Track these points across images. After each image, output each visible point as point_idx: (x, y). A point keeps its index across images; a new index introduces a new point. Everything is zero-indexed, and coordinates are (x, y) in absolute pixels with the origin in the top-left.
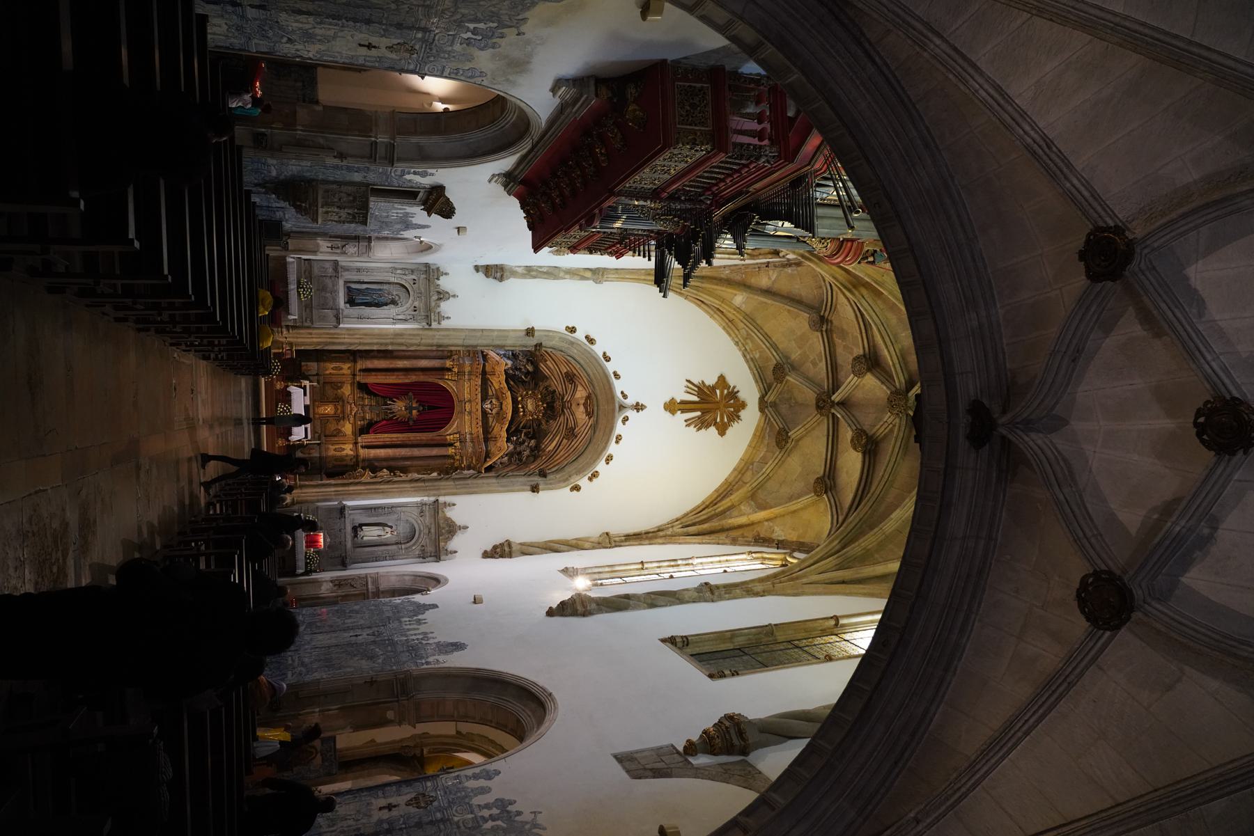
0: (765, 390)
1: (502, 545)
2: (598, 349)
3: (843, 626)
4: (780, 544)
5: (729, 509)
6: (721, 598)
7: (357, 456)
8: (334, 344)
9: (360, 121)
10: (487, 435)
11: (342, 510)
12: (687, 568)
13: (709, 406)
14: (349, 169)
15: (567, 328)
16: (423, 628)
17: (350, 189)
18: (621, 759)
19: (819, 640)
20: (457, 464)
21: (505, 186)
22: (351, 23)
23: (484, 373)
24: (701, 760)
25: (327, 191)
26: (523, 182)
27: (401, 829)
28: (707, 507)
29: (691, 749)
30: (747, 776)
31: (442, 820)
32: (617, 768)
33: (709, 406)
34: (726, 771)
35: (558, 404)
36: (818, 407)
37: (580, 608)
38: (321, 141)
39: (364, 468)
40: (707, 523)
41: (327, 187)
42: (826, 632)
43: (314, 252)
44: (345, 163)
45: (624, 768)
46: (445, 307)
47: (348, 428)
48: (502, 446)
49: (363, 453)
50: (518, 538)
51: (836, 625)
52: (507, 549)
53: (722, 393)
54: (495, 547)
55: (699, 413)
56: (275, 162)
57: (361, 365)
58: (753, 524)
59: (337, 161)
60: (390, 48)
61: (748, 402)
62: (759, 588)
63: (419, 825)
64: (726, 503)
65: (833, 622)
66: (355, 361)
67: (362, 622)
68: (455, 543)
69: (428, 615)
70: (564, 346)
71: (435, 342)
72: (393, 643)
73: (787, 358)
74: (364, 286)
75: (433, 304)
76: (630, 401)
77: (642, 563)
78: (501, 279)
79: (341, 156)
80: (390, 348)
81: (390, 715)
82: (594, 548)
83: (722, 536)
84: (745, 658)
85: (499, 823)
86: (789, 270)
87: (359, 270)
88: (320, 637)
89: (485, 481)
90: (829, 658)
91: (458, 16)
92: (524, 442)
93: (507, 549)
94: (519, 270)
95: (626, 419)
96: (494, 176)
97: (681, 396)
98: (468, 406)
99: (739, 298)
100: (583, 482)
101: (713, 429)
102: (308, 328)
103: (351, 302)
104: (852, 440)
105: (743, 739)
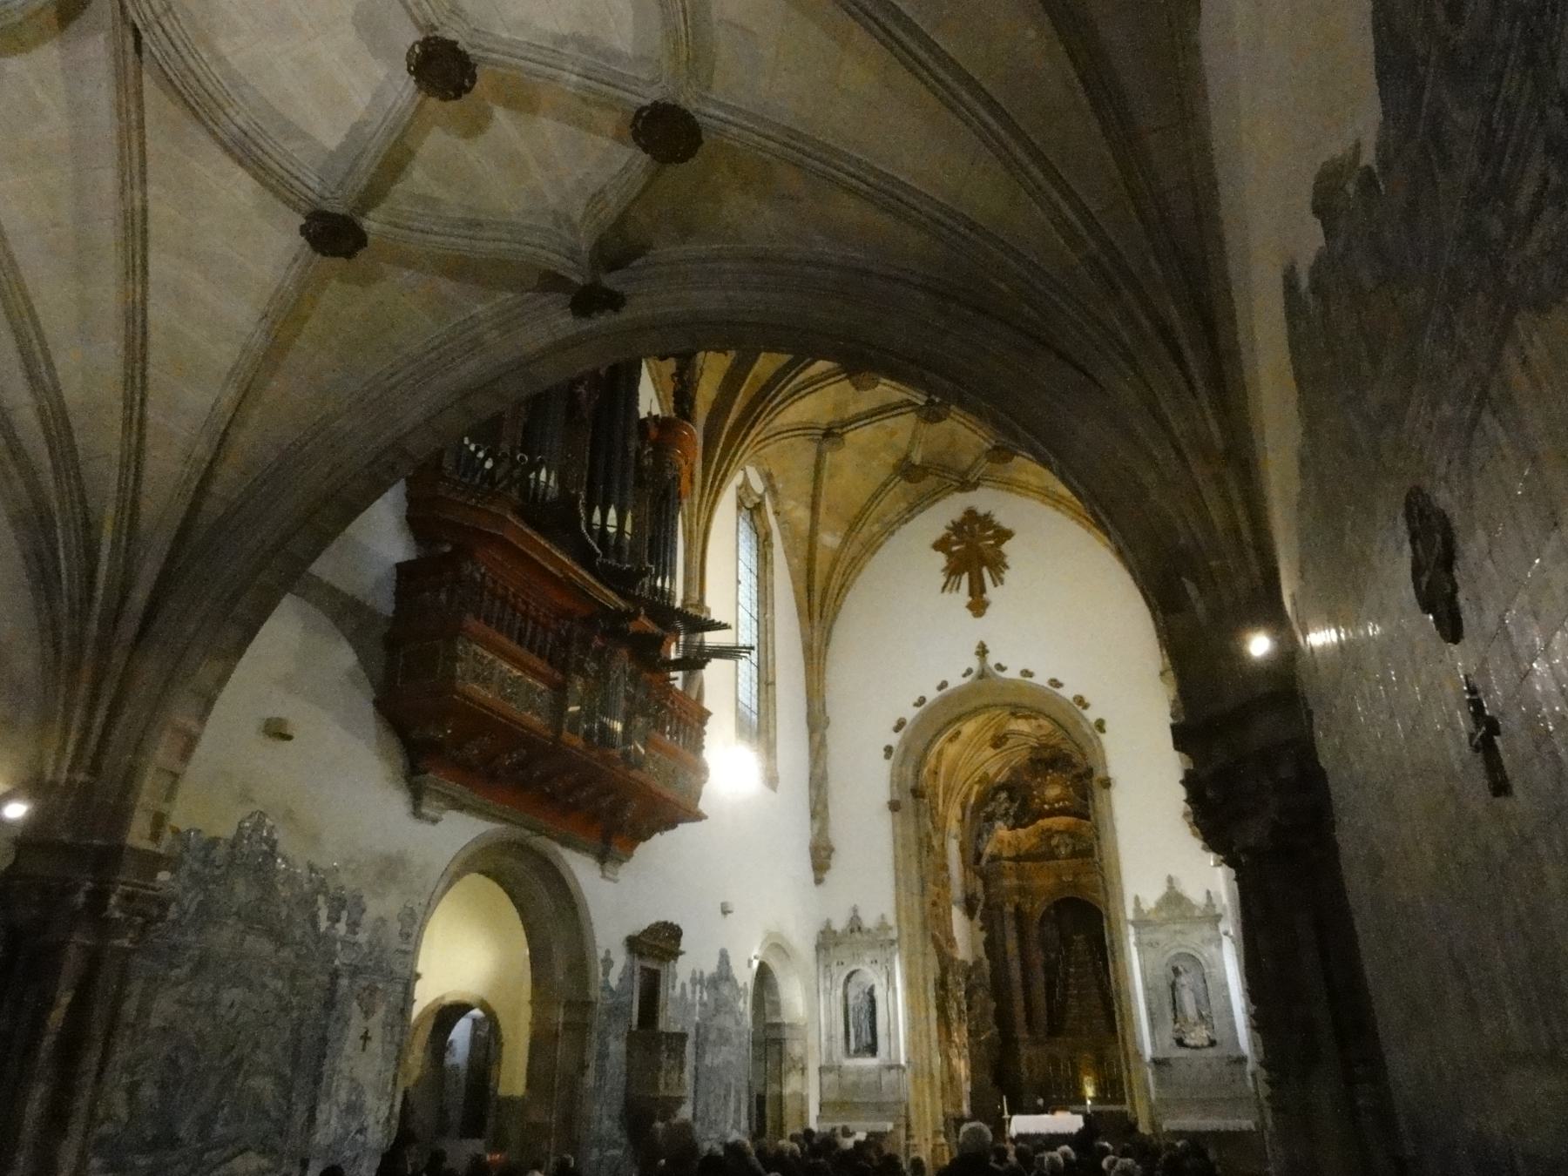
2: (910, 714)
9: (541, 1043)
11: (1158, 1063)
13: (974, 556)
14: (603, 1056)
15: (887, 757)
21: (621, 862)
22: (326, 1061)
23: (1017, 859)
33: (974, 556)
35: (1046, 754)
43: (803, 1100)
44: (592, 1064)
46: (869, 921)
55: (985, 571)
56: (595, 1151)
57: (1022, 1033)
60: (368, 1013)
61: (965, 508)
66: (1016, 1041)
68: (1196, 896)
74: (852, 1031)
76: (974, 663)
78: (830, 850)
79: (582, 1067)
86: (780, 486)
87: (830, 1038)
91: (308, 940)
94: (817, 826)
95: (1000, 667)
96: (604, 876)
97: (963, 596)
98: (1067, 878)
99: (829, 540)
100: (1091, 715)
101: (1006, 547)
102: (907, 1108)
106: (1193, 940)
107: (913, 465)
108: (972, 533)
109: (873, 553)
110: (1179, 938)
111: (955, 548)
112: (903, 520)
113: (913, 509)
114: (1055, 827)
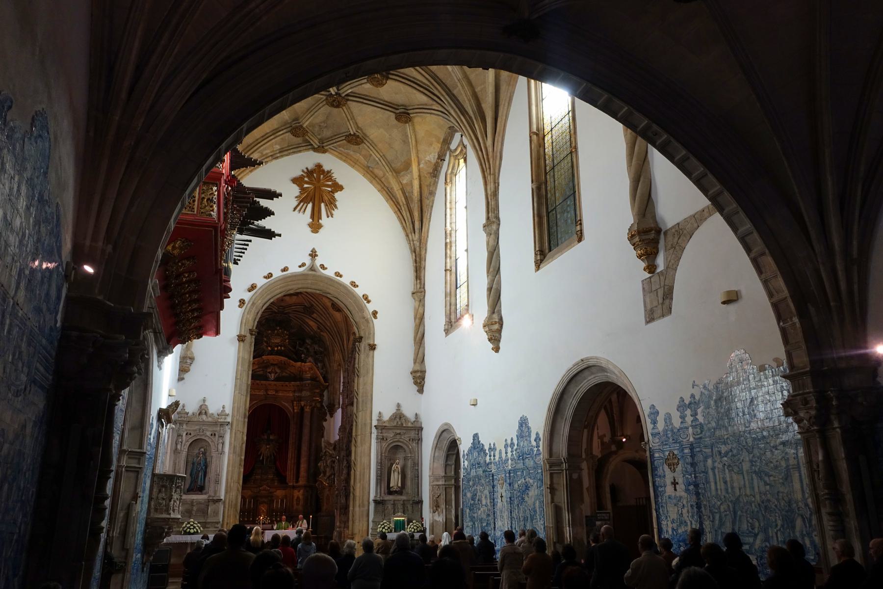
0: (309, 146)
1: (414, 378)
2: (261, 282)
3: (538, 129)
4: (441, 158)
5: (404, 193)
6: (498, 218)
7: (305, 487)
8: (236, 505)
10: (297, 377)
12: (453, 235)
15: (240, 306)
16: (500, 446)
17: (155, 490)
18: (650, 318)
19: (548, 150)
20: (318, 405)
24: (660, 262)
25: (156, 510)
26: (168, 341)
27: (695, 477)
29: (651, 268)
30: (684, 232)
31: (692, 447)
32: (660, 324)
33: (318, 193)
34: (673, 247)
36: (338, 106)
37: (496, 327)
38: (122, 515)
39: (316, 481)
40: (414, 214)
41: (152, 510)
42: (541, 144)
45: (660, 317)
46: (214, 408)
47: (280, 493)
48: (308, 366)
49: (302, 482)
50: (409, 364)
51: (537, 135)
52: (419, 374)
53: (307, 183)
54: (416, 383)
55: (323, 205)
58: (420, 176)
59: (139, 500)
62: (491, 186)
63: (693, 465)
65: (535, 137)
67: (486, 492)
69: (486, 441)
70: (254, 310)
72: (515, 471)
73: (286, 123)
75: (210, 419)
76: (308, 262)
77: (446, 270)
79: (135, 497)
80: (243, 458)
81: (575, 476)
82: (424, 306)
83: (426, 202)
84: (559, 210)
85: (699, 411)
88: (499, 524)
89: (361, 388)
90: (573, 151)
92: (307, 349)
93: (419, 374)
95: (323, 267)
97: (306, 217)
100: (371, 308)
101: (337, 195)
103: (201, 489)
104: (376, 86)
105: (650, 230)
106: (405, 438)
107: (301, 126)
108: (319, 179)
110: (398, 437)
111: (306, 186)
112: (274, 157)
113: (285, 151)
114: (272, 362)
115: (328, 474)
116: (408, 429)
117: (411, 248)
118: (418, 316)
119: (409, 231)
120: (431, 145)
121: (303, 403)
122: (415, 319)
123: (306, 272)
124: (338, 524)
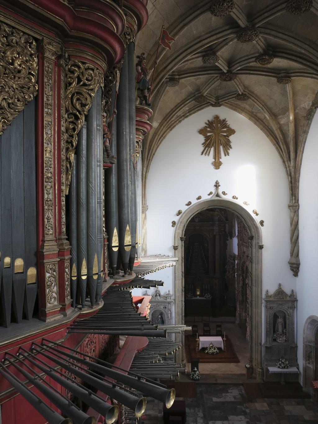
15: (173, 226)
28: (278, 143)
33: (217, 139)
53: (209, 132)
55: (221, 147)
64: (278, 133)
68: (288, 291)
71: (181, 293)
76: (213, 190)
80: (184, 314)
82: (298, 216)
83: (301, 138)
89: (254, 270)
93: (295, 266)
95: (224, 193)
97: (210, 158)
101: (231, 138)
107: (202, 96)
109: (171, 130)
111: (209, 134)
112: (185, 116)
113: (191, 111)
115: (231, 273)
116: (287, 302)
117: (287, 171)
118: (294, 223)
119: (285, 159)
120: (307, 95)
121: (215, 233)
122: (291, 224)
123: (213, 198)
124: (239, 309)
